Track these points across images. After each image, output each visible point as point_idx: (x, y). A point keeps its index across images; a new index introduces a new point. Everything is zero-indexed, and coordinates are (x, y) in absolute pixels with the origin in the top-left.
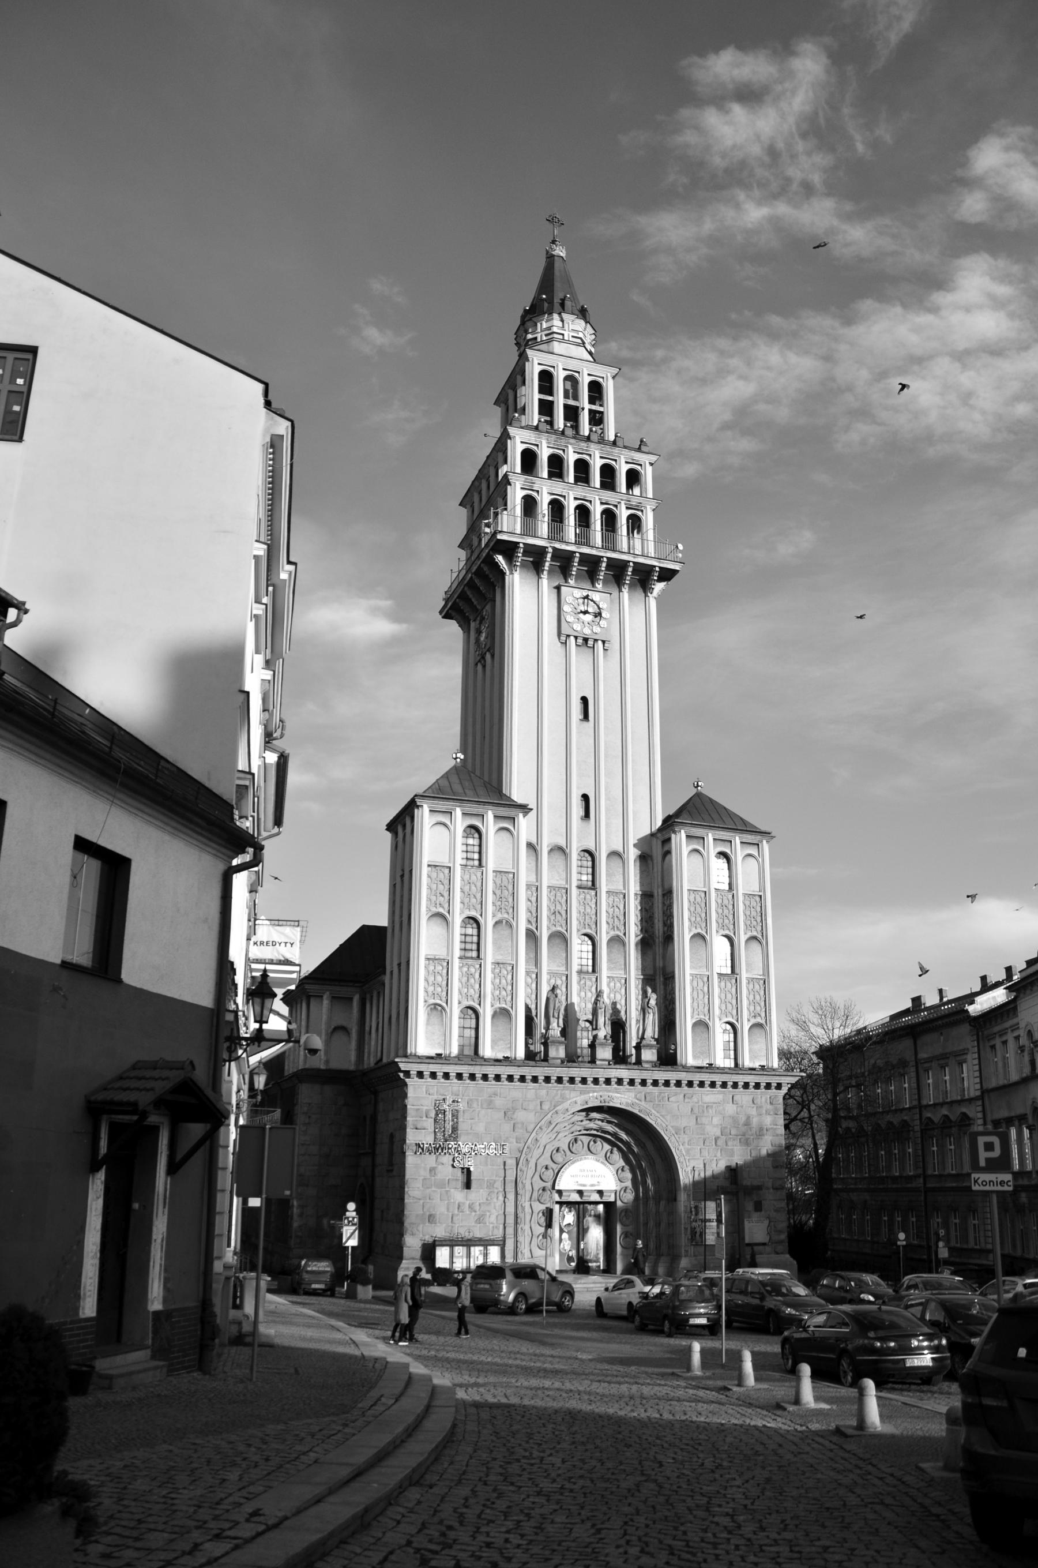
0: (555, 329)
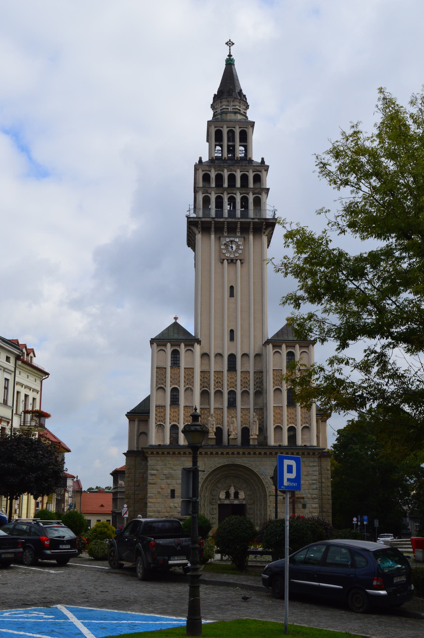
0: (224, 107)
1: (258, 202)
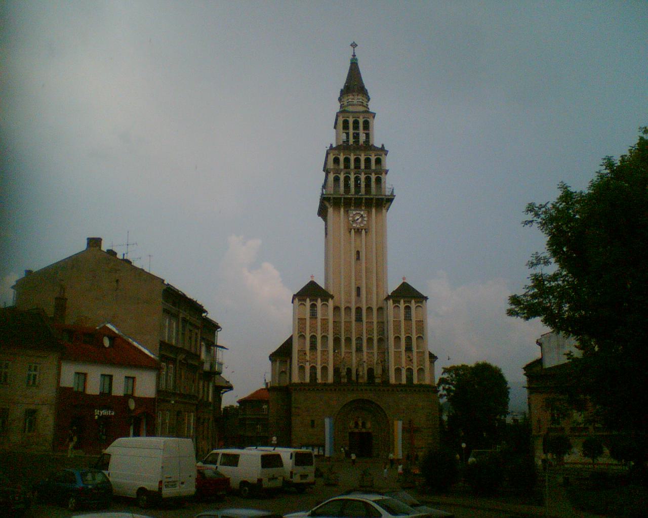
0: (350, 100)
1: (379, 181)
